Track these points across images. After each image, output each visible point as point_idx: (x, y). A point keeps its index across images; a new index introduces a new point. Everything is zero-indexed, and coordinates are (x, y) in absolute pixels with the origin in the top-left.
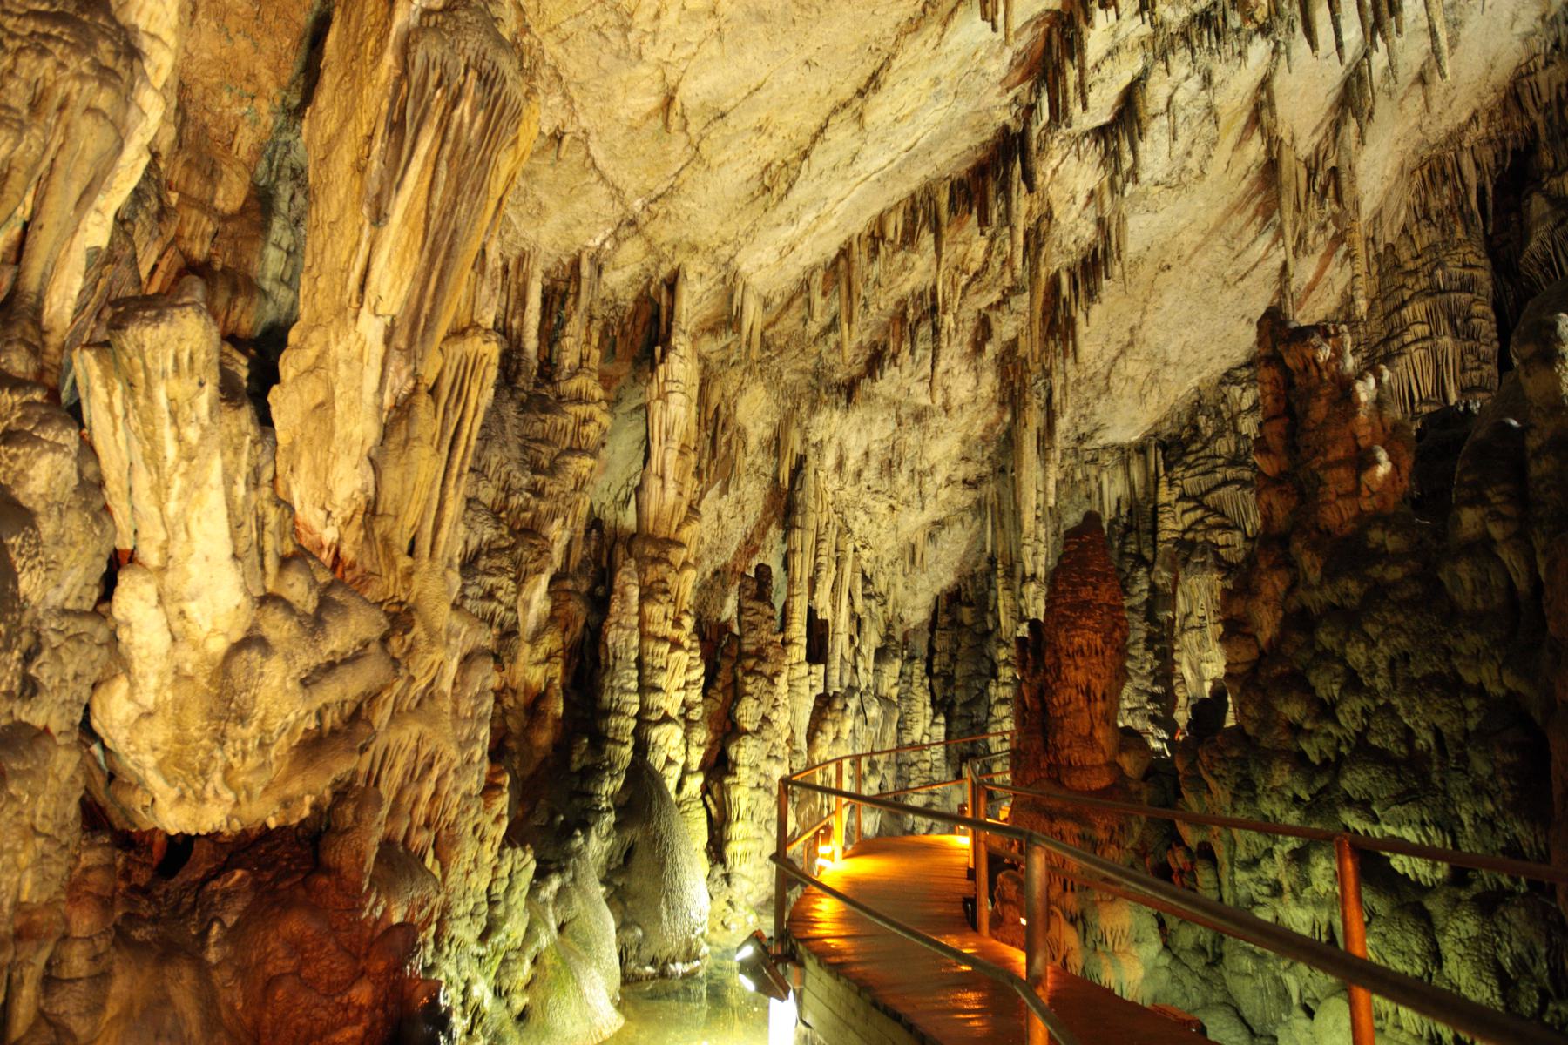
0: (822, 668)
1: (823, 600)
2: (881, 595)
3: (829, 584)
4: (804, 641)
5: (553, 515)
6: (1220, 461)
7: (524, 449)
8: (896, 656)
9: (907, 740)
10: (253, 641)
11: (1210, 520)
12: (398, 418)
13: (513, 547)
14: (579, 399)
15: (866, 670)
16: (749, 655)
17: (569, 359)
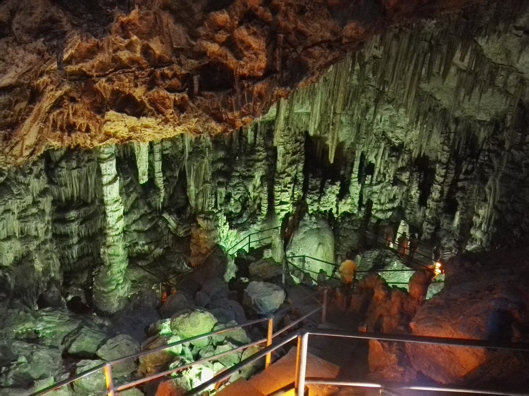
0: (370, 177)
1: (371, 159)
2: (410, 150)
3: (374, 155)
4: (357, 173)
5: (253, 173)
6: (497, 143)
7: (246, 164)
8: (408, 171)
9: (410, 194)
10: (177, 228)
11: (487, 162)
12: (197, 196)
13: (243, 182)
14: (259, 151)
15: (389, 176)
16: (310, 189)
17: (257, 143)
